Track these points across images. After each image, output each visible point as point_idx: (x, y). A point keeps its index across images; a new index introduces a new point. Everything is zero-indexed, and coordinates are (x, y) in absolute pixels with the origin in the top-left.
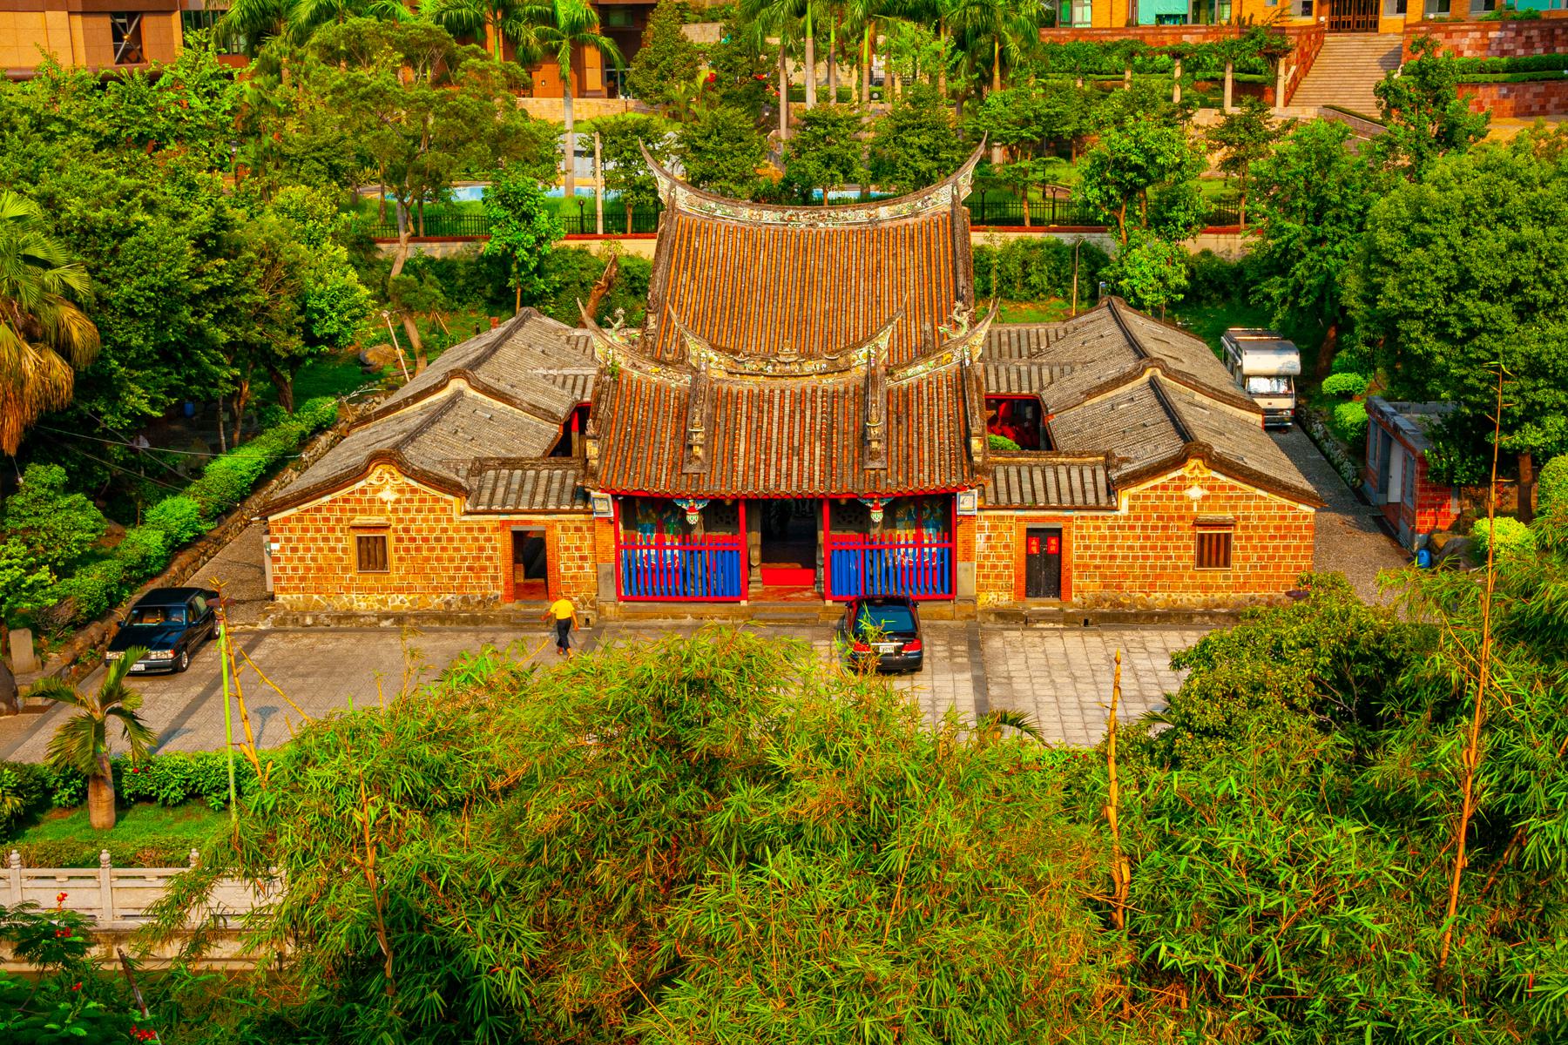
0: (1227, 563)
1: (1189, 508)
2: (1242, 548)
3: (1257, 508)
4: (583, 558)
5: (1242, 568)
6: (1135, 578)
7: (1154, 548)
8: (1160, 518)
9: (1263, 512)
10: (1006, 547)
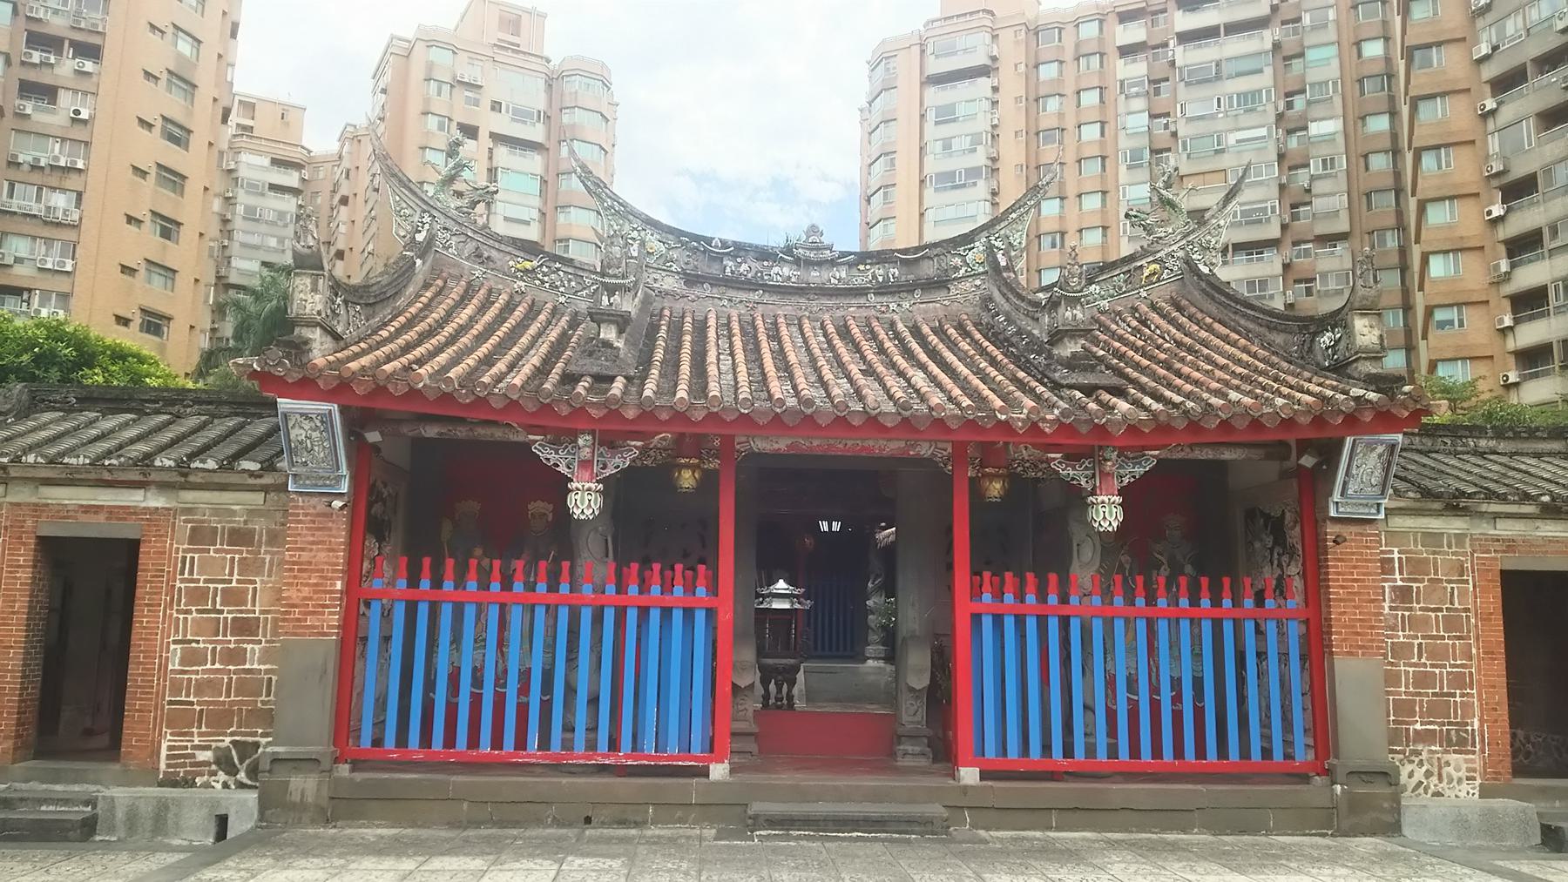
4: (245, 627)
10: (1452, 623)
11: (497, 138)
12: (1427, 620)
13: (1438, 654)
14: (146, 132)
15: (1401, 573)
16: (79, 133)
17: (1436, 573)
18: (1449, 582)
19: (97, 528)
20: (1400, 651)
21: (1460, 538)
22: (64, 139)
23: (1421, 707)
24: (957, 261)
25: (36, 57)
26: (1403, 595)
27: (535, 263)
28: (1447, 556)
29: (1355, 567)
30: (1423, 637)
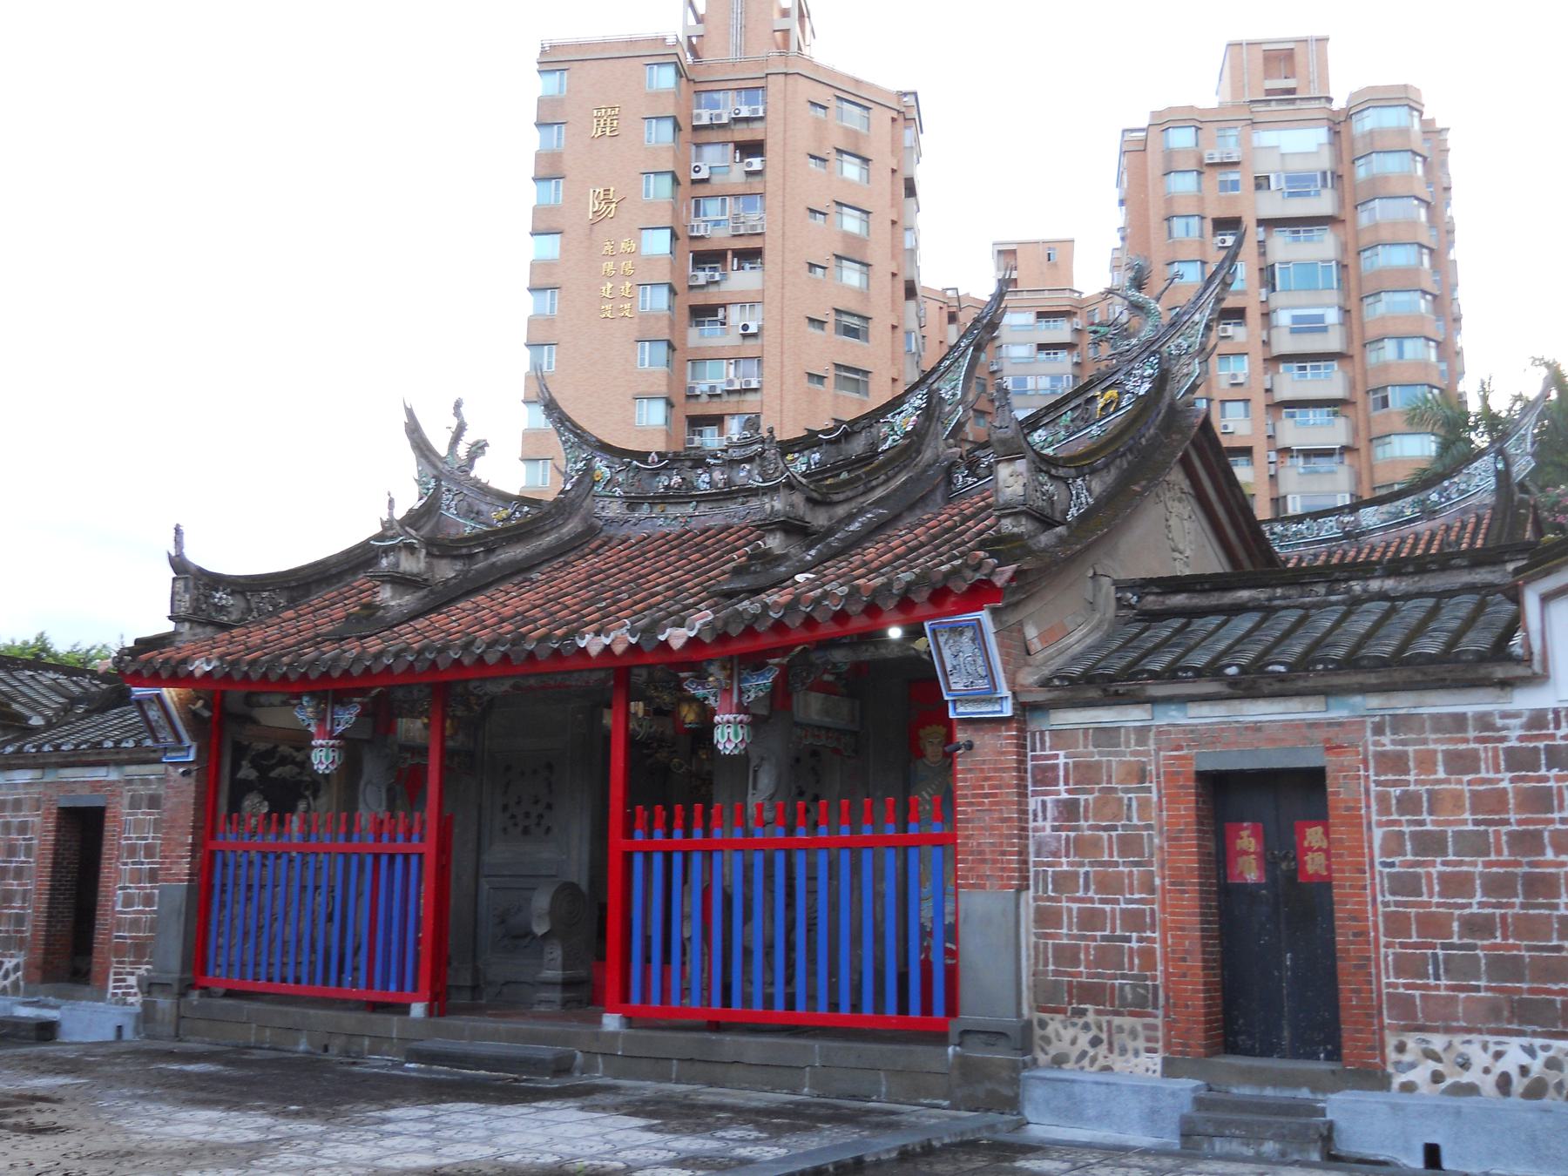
10: (1129, 845)
11: (1268, 223)
13: (1109, 885)
14: (818, 332)
15: (1066, 783)
16: (751, 348)
17: (1109, 781)
18: (1127, 791)
19: (85, 799)
20: (1064, 882)
21: (1142, 732)
22: (737, 360)
24: (885, 429)
25: (702, 277)
26: (1069, 810)
27: (510, 511)
28: (1129, 753)
29: (987, 779)
30: (1092, 864)
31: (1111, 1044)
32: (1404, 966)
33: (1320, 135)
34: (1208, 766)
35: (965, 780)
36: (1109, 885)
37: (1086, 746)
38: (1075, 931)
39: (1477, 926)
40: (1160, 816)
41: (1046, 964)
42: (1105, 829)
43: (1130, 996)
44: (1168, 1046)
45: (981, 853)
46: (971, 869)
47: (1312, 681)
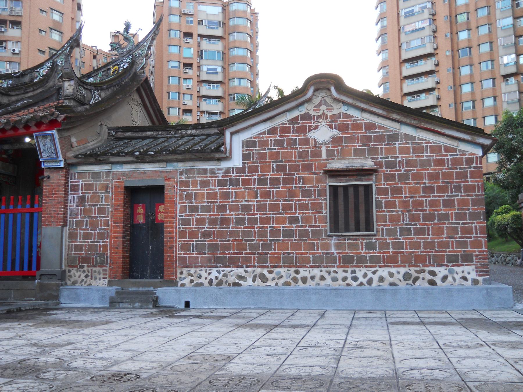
0: (369, 227)
1: (317, 154)
2: (389, 205)
3: (404, 151)
5: (391, 232)
6: (254, 248)
7: (274, 207)
8: (281, 168)
9: (412, 156)
10: (101, 211)
11: (201, 36)
12: (90, 210)
13: (94, 224)
14: (42, 55)
15: (82, 190)
16: (16, 58)
17: (96, 190)
20: (79, 224)
21: (108, 174)
22: (10, 62)
23: (85, 247)
26: (82, 200)
28: (103, 180)
29: (54, 189)
30: (89, 217)
31: (92, 277)
32: (184, 248)
33: (219, 9)
34: (128, 185)
35: (46, 189)
36: (94, 224)
37: (89, 178)
38: (82, 240)
39: (206, 235)
40: (112, 201)
41: (72, 251)
42: (94, 206)
43: (99, 261)
44: (110, 276)
45: (51, 214)
46: (47, 219)
47: (161, 157)
